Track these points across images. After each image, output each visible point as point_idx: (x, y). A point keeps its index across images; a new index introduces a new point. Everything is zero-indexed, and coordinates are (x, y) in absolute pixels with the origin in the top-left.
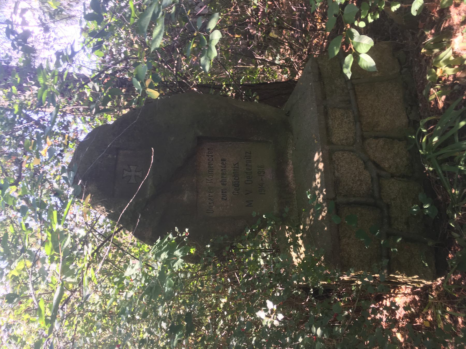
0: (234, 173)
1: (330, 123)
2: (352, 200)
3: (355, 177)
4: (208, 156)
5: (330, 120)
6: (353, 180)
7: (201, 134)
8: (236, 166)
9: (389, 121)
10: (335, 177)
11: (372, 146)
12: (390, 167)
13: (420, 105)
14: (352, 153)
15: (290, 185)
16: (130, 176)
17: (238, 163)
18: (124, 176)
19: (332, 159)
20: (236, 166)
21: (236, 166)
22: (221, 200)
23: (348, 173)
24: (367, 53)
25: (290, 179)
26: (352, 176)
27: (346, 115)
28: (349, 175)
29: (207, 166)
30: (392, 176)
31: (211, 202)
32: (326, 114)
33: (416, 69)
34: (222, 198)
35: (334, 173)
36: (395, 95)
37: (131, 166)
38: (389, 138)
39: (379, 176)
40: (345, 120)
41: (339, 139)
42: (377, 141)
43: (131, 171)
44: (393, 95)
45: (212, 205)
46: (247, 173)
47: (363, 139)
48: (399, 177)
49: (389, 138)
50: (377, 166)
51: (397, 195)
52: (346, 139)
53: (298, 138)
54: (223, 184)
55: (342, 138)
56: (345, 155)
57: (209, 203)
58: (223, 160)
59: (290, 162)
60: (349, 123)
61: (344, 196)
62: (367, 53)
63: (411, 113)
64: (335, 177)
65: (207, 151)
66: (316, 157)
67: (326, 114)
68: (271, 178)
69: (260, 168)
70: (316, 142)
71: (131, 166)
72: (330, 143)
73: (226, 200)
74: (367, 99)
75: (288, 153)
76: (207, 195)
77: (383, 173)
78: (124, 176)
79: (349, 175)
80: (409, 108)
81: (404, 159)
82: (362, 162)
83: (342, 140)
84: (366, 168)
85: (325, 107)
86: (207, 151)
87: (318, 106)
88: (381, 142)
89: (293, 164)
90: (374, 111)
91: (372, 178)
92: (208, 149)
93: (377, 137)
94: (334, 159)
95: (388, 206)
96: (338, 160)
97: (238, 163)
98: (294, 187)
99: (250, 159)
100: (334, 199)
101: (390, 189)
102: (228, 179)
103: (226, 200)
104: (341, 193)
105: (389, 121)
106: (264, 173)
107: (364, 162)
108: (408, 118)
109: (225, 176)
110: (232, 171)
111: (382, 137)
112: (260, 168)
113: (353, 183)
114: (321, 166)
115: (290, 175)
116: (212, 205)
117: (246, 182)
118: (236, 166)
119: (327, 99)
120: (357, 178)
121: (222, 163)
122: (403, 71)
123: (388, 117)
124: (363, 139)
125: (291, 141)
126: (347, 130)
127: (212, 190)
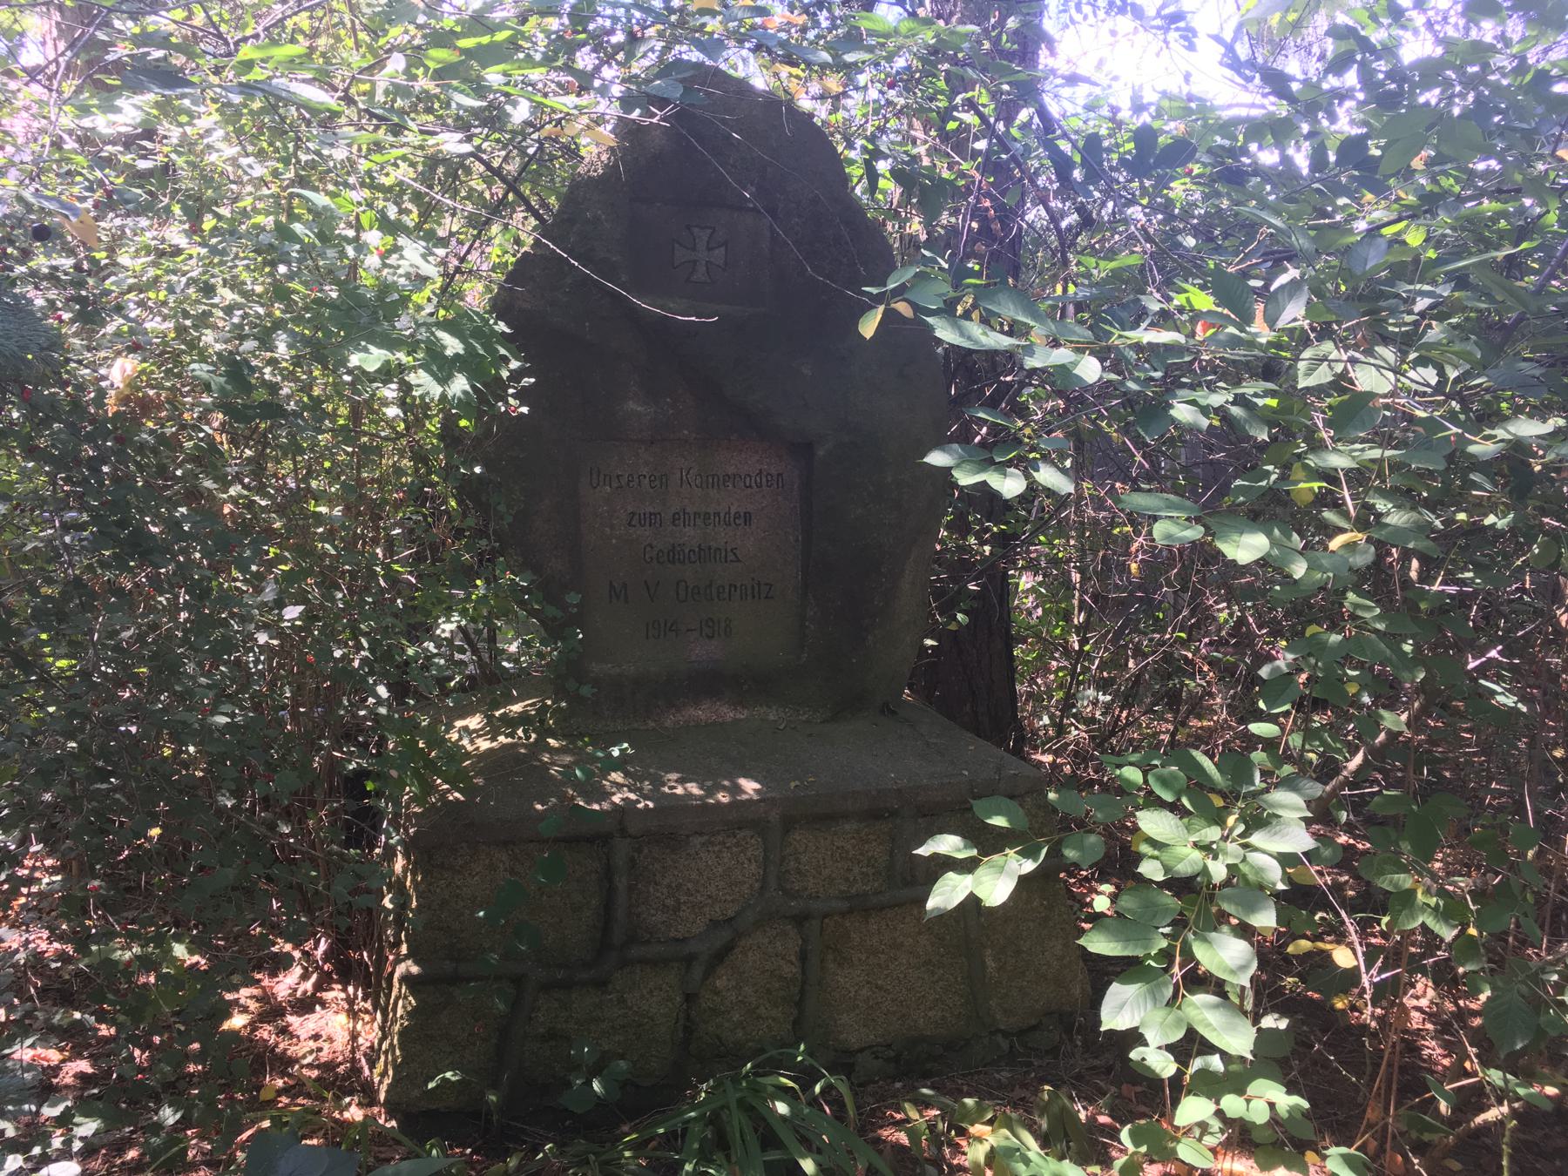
1: (847, 827)
2: (621, 883)
3: (689, 893)
5: (855, 827)
6: (679, 886)
7: (821, 453)
9: (852, 995)
10: (688, 836)
11: (778, 944)
12: (717, 993)
13: (898, 1085)
14: (757, 885)
15: (673, 710)
16: (694, 249)
17: (739, 561)
18: (696, 230)
19: (740, 828)
21: (730, 554)
22: (630, 509)
23: (701, 874)
24: (972, 895)
25: (692, 712)
26: (690, 885)
27: (871, 871)
28: (694, 876)
29: (731, 470)
30: (689, 998)
31: (624, 481)
32: (874, 815)
33: (1004, 1075)
34: (633, 514)
35: (701, 834)
36: (930, 1014)
37: (723, 249)
38: (802, 992)
39: (689, 960)
40: (856, 870)
41: (801, 850)
42: (793, 958)
43: (709, 249)
44: (931, 1009)
45: (615, 485)
46: (710, 585)
47: (800, 920)
48: (688, 1018)
49: (802, 992)
50: (721, 956)
51: (635, 1009)
52: (799, 872)
53: (810, 735)
54: (675, 519)
55: (804, 859)
56: (753, 866)
57: (618, 476)
58: (747, 518)
59: (743, 715)
60: (847, 880)
61: (632, 860)
62: (972, 895)
63: (877, 1058)
64: (688, 836)
66: (750, 786)
67: (874, 815)
68: (693, 658)
69: (723, 625)
70: (793, 785)
71: (723, 249)
72: (789, 823)
73: (630, 524)
74: (920, 933)
75: (770, 707)
77: (698, 971)
78: (696, 230)
79: (694, 876)
80: (892, 1054)
81: (740, 1033)
82: (731, 913)
83: (797, 860)
84: (714, 924)
85: (894, 814)
86: (774, 472)
87: (899, 790)
88: (790, 970)
89: (736, 721)
90: (883, 953)
91: (684, 940)
93: (803, 957)
94: (741, 834)
95: (601, 984)
96: (737, 845)
97: (739, 561)
98: (668, 723)
100: (623, 832)
101: (651, 992)
103: (630, 524)
104: (639, 851)
105: (852, 995)
106: (710, 637)
107: (731, 919)
108: (861, 1050)
111: (804, 973)
112: (723, 625)
113: (669, 886)
114: (723, 797)
115: (701, 713)
116: (615, 485)
118: (730, 554)
119: (920, 820)
120: (683, 899)
122: (999, 1038)
123: (865, 992)
124: (800, 920)
125: (804, 718)
126: (826, 872)
127: (657, 483)
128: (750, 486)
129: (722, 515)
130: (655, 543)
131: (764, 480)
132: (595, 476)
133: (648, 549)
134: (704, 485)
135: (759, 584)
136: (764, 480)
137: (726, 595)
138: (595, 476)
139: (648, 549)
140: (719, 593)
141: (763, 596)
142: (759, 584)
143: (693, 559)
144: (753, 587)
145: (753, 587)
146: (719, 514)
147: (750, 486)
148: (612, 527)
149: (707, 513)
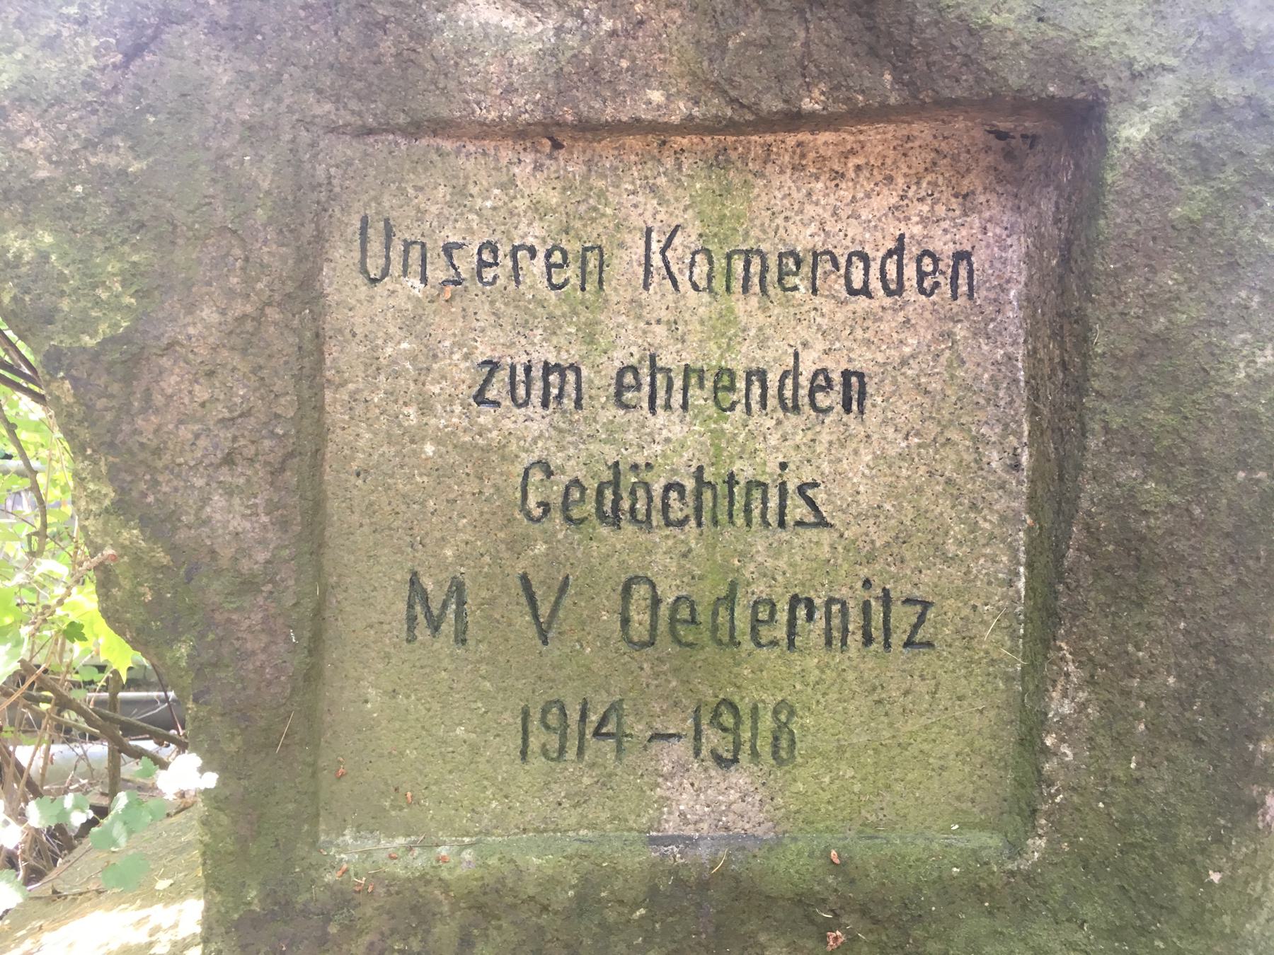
0: (731, 480)
4: (898, 250)
8: (795, 509)
17: (822, 523)
20: (795, 509)
21: (794, 503)
22: (483, 351)
29: (804, 238)
31: (466, 265)
45: (438, 272)
46: (730, 599)
57: (448, 249)
65: (944, 246)
68: (671, 827)
69: (767, 722)
73: (480, 399)
76: (533, 233)
86: (944, 246)
92: (961, 257)
97: (822, 523)
99: (855, 640)
102: (667, 424)
103: (480, 399)
109: (698, 397)
110: (745, 470)
112: (767, 722)
116: (438, 272)
117: (641, 591)
118: (794, 503)
121: (821, 384)
127: (572, 272)
128: (866, 291)
129: (773, 378)
130: (556, 460)
131: (910, 271)
132: (375, 246)
133: (537, 476)
134: (719, 284)
135: (886, 599)
136: (910, 271)
137: (781, 633)
138: (375, 246)
139: (537, 476)
140: (756, 623)
141: (897, 639)
142: (886, 599)
143: (676, 515)
144: (866, 608)
145: (866, 608)
146: (762, 375)
147: (866, 291)
148: (425, 407)
149: (721, 372)
